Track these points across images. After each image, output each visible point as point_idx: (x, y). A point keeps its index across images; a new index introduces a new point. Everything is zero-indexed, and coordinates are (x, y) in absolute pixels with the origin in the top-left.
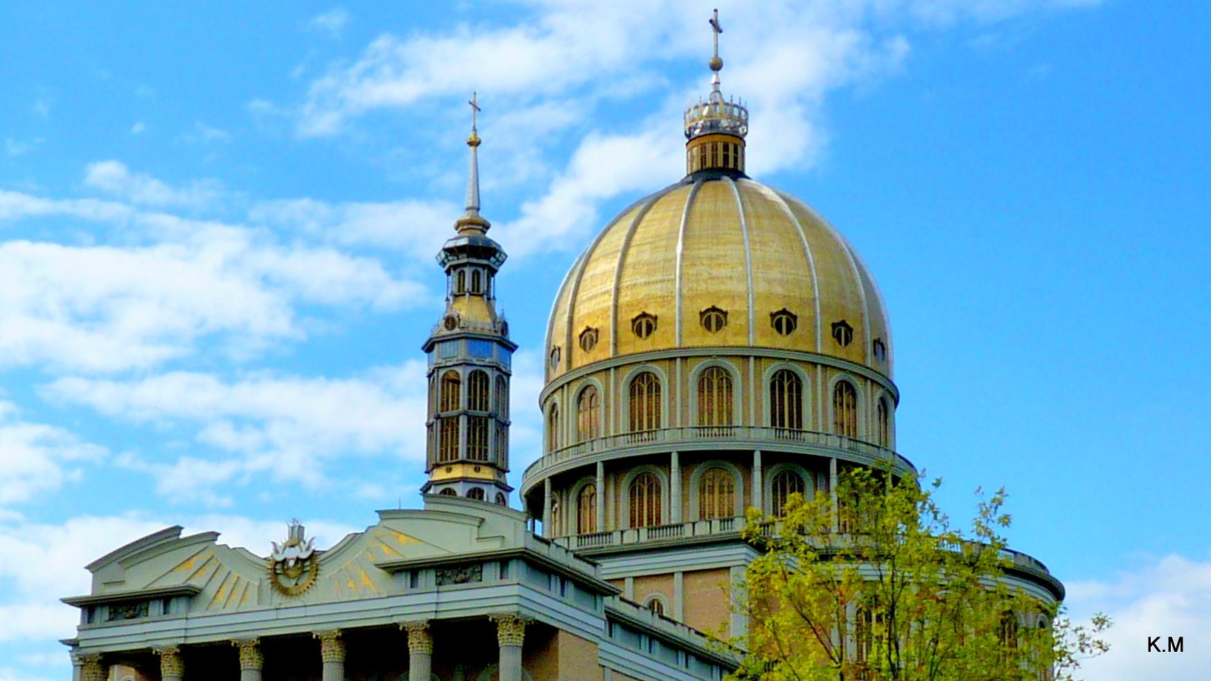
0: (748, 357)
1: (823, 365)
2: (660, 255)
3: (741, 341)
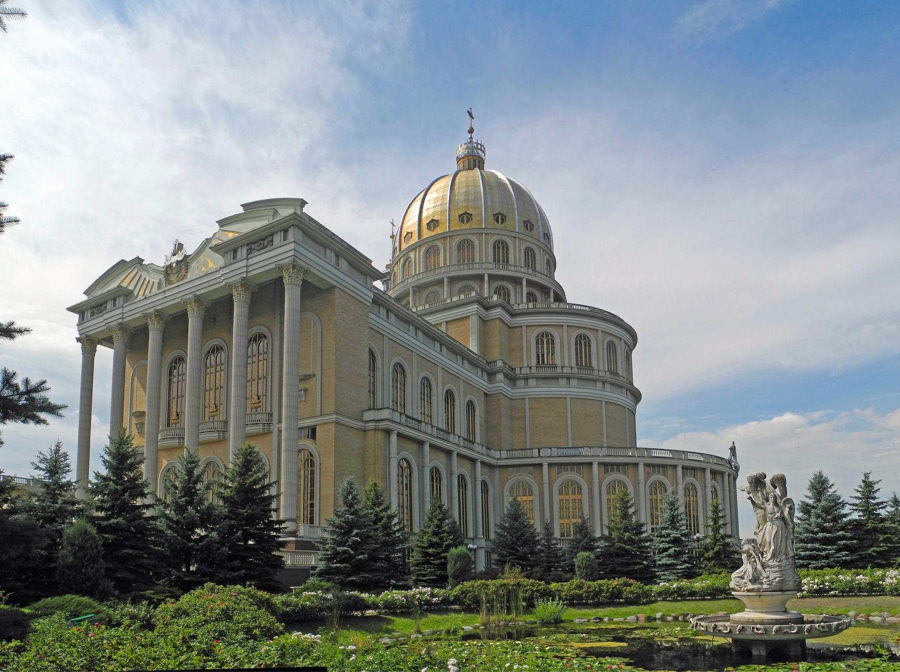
2: (441, 194)
3: (478, 226)
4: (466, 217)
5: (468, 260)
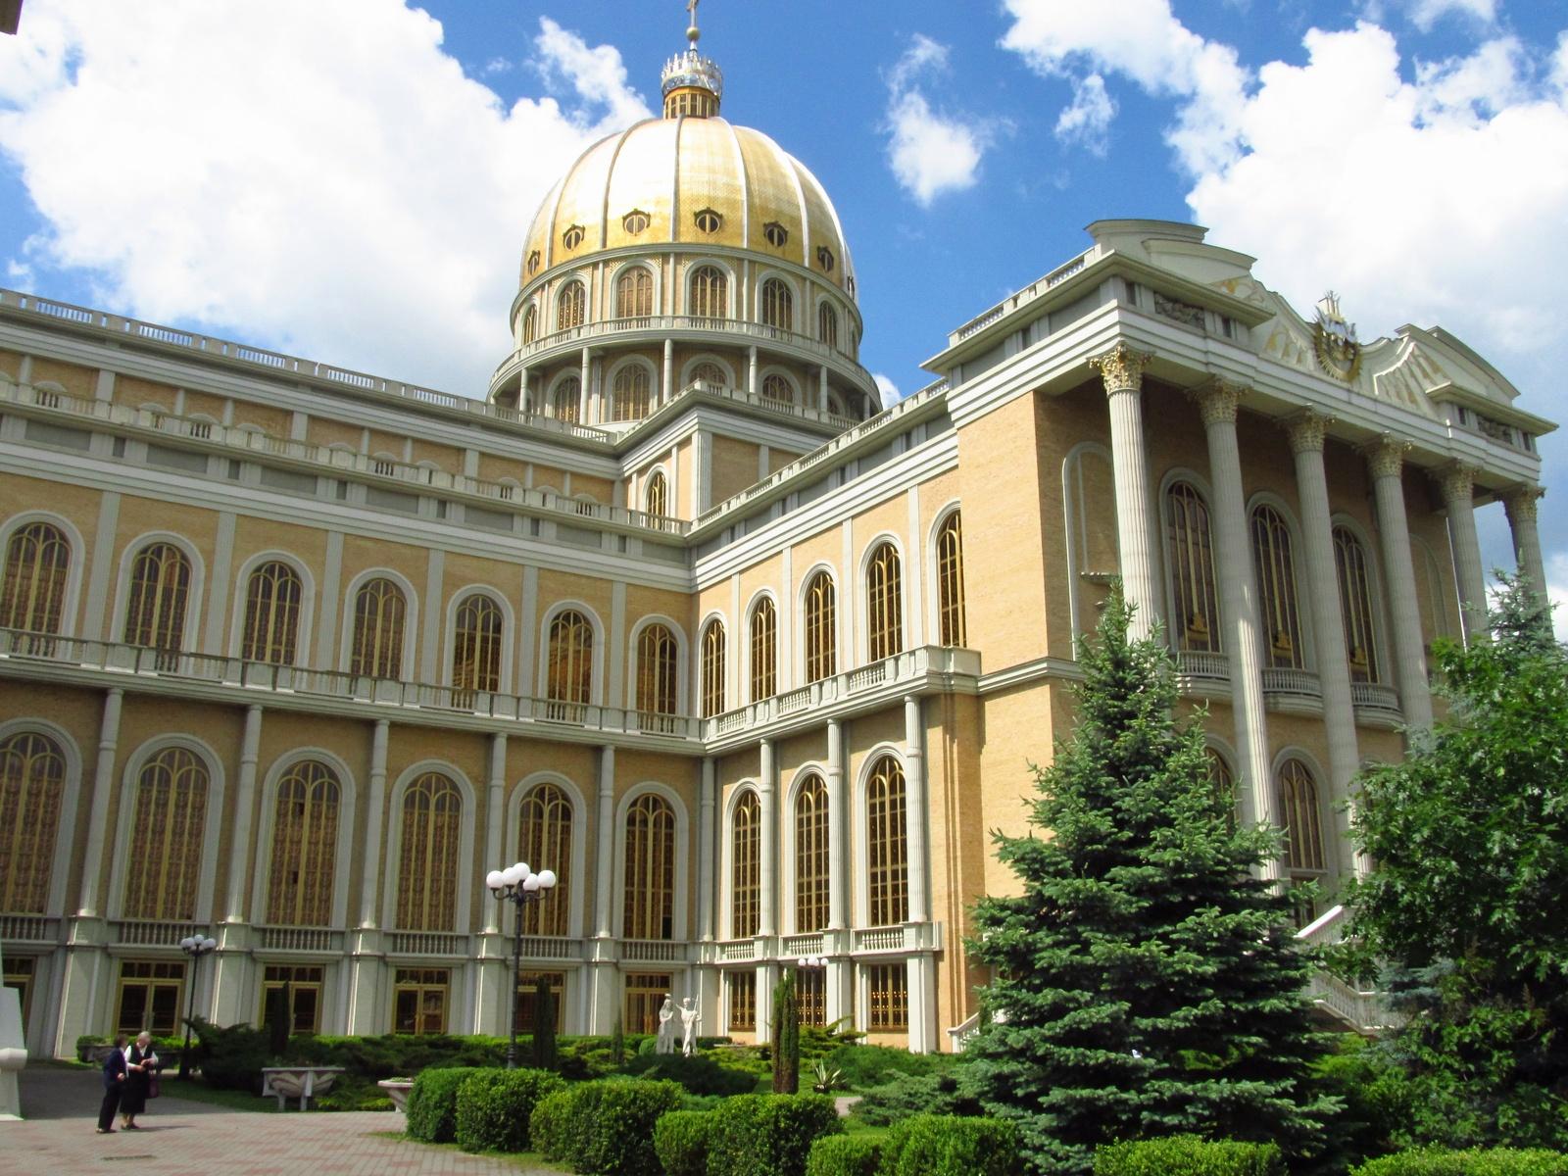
0: (742, 260)
1: (813, 283)
4: (708, 219)
5: (713, 313)
